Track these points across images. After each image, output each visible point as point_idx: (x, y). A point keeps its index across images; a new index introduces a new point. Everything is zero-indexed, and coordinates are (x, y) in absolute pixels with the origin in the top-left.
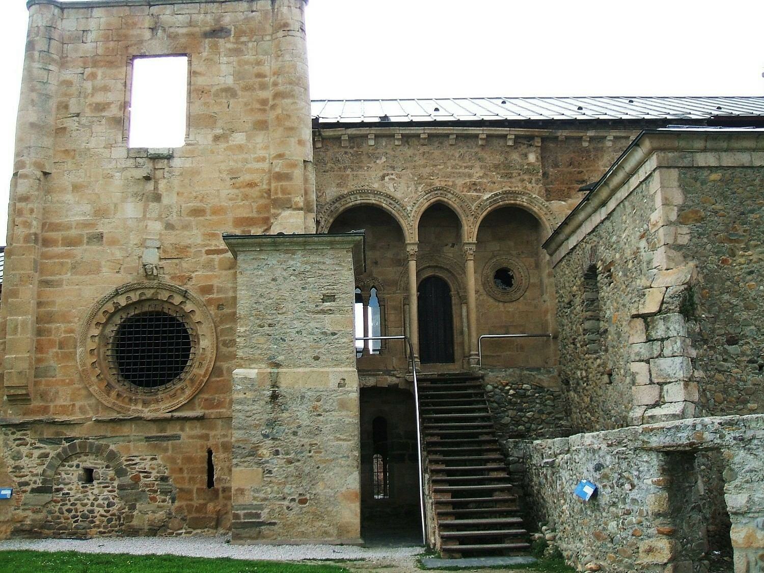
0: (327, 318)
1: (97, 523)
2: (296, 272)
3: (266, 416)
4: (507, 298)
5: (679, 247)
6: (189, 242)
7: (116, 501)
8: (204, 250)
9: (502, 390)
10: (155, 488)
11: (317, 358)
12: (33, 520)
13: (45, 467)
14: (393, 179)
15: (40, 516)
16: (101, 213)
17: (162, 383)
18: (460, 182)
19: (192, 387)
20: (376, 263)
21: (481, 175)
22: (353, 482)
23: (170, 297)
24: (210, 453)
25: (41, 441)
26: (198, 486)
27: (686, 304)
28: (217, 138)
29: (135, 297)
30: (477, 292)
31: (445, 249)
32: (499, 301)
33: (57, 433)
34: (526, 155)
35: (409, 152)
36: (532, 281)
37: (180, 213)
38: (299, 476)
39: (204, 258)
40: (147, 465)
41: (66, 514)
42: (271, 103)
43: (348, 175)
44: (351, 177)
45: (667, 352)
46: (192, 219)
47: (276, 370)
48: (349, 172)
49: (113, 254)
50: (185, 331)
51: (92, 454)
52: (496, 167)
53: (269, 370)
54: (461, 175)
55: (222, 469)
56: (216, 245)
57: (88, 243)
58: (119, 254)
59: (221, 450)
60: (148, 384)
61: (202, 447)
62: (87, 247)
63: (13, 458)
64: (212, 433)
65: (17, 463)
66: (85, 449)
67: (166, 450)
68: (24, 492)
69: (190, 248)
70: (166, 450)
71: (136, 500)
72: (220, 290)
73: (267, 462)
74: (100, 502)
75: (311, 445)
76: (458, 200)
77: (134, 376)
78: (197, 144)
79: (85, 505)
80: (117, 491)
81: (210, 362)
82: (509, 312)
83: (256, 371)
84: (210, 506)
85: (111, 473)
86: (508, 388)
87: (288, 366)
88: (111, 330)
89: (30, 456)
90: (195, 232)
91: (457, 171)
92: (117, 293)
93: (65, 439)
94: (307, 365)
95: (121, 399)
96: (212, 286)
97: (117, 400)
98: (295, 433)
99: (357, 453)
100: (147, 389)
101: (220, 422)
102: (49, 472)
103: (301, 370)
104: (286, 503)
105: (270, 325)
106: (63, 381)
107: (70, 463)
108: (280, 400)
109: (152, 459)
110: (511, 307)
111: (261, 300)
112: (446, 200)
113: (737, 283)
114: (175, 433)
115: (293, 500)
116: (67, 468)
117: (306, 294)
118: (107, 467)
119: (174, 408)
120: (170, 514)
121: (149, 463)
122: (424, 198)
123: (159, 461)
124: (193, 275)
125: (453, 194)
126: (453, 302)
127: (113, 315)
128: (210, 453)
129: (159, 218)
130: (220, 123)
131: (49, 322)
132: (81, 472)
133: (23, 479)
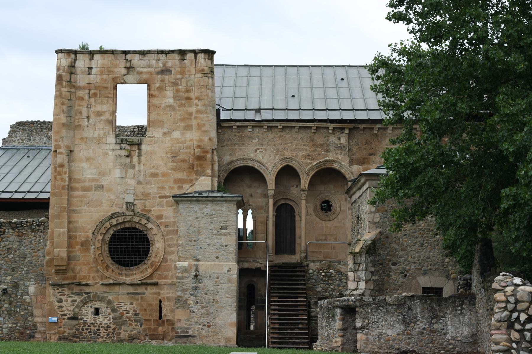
0: (223, 238)
1: (102, 336)
2: (208, 215)
3: (192, 285)
4: (327, 219)
5: (374, 223)
6: (150, 191)
7: (111, 325)
8: (158, 196)
9: (318, 273)
10: (132, 319)
11: (217, 258)
12: (69, 333)
13: (74, 307)
14: (262, 152)
15: (72, 331)
16: (102, 174)
17: (135, 265)
18: (300, 154)
20: (251, 196)
22: (233, 317)
23: (140, 220)
24: (160, 302)
25: (72, 293)
26: (154, 318)
27: (371, 249)
28: (164, 134)
29: (121, 220)
31: (292, 188)
33: (81, 290)
34: (339, 139)
35: (271, 135)
37: (145, 175)
38: (207, 314)
39: (158, 200)
40: (128, 307)
41: (85, 331)
42: (194, 115)
43: (236, 149)
44: (238, 150)
45: (361, 269)
46: (151, 179)
47: (197, 263)
48: (237, 147)
49: (109, 197)
50: (147, 238)
51: (99, 300)
53: (194, 263)
54: (301, 150)
55: (167, 310)
57: (95, 190)
58: (113, 197)
59: (166, 301)
60: (128, 266)
61: (156, 299)
63: (58, 302)
64: (162, 292)
65: (60, 304)
66: (96, 298)
67: (137, 300)
68: (64, 319)
70: (137, 300)
71: (122, 325)
73: (192, 307)
74: (103, 325)
75: (214, 300)
76: (298, 165)
77: (121, 261)
78: (154, 137)
79: (95, 327)
80: (112, 320)
83: (187, 263)
84: (160, 329)
85: (109, 310)
87: (203, 261)
88: (108, 237)
89: (66, 301)
90: (153, 186)
91: (299, 147)
92: (112, 217)
93: (85, 293)
94: (213, 261)
96: (162, 215)
98: (206, 294)
99: (235, 304)
100: (128, 268)
101: (166, 286)
102: (77, 310)
103: (209, 263)
104: (201, 326)
105: (195, 241)
106: (84, 263)
107: (87, 305)
108: (199, 277)
109: (130, 304)
110: (329, 224)
111: (191, 228)
112: (291, 164)
113: (399, 239)
115: (204, 325)
116: (86, 308)
117: (212, 226)
118: (107, 308)
120: (140, 332)
121: (128, 306)
123: (134, 305)
124: (152, 209)
127: (109, 229)
128: (160, 302)
129: (134, 178)
130: (166, 125)
131: (75, 232)
132: (93, 310)
133: (63, 313)
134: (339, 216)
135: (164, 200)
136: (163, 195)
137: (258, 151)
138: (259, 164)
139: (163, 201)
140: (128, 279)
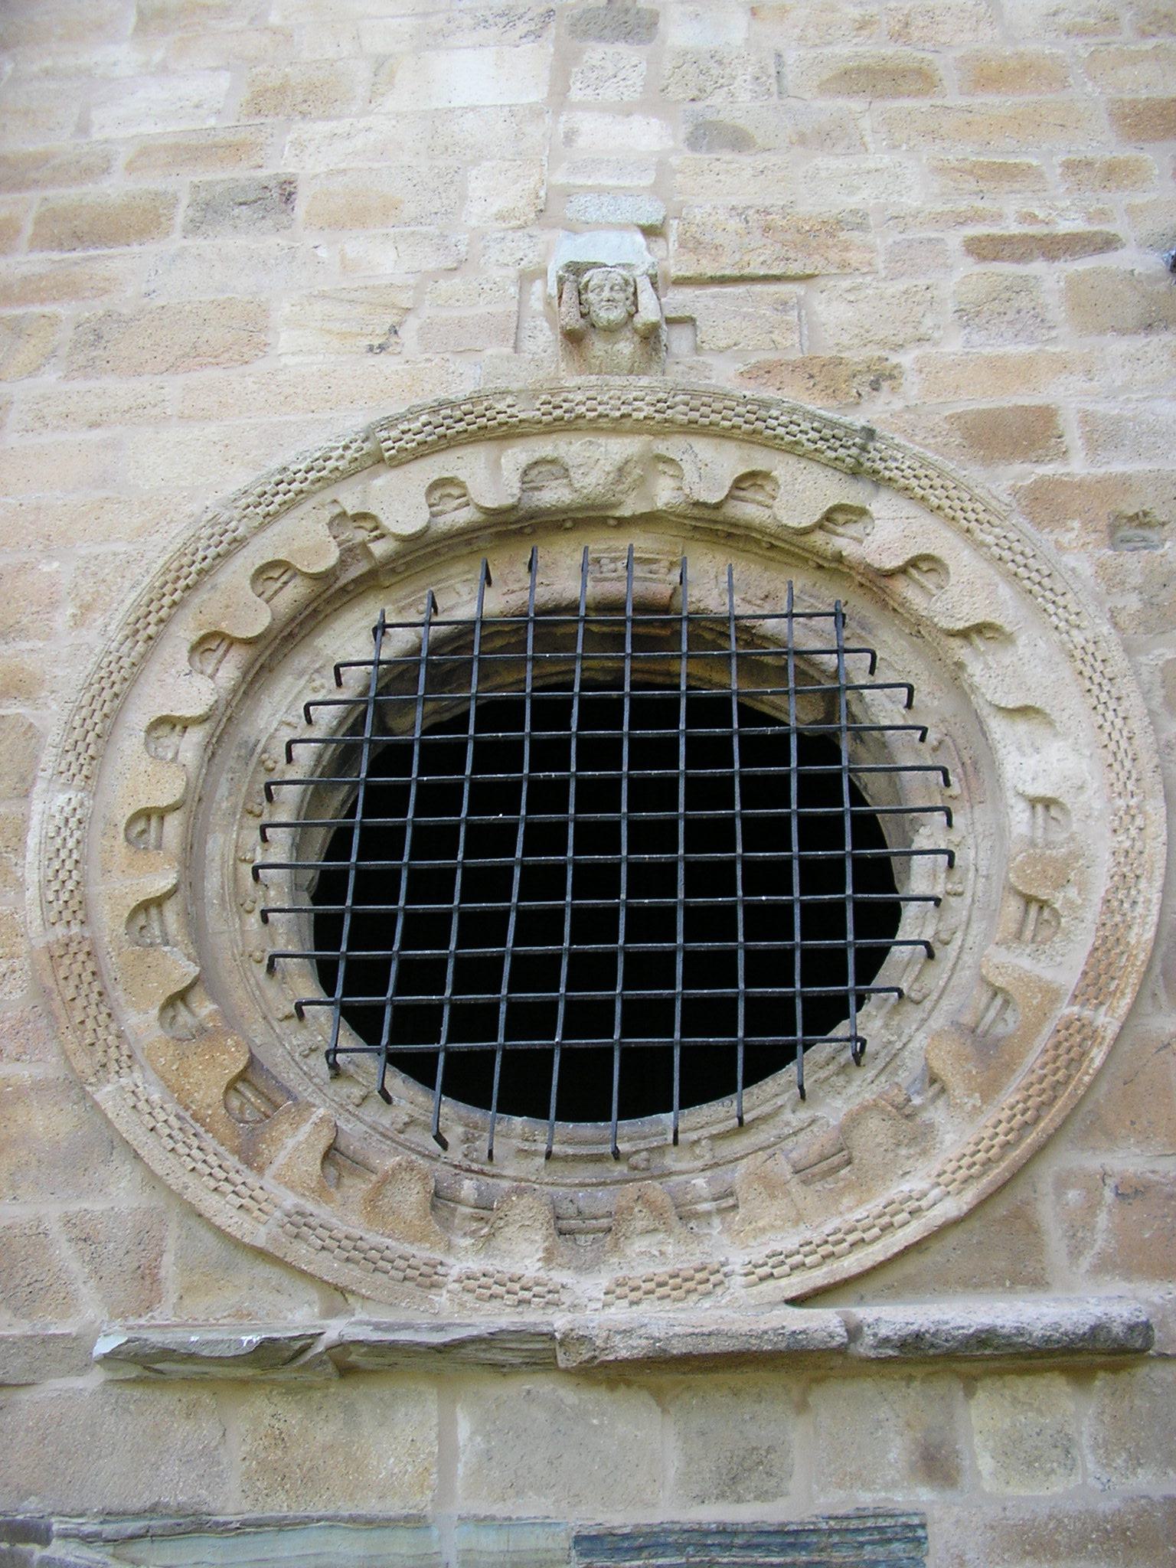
6: (853, 202)
19: (989, 1090)
29: (491, 479)
46: (856, 105)
56: (1032, 218)
57: (194, 227)
62: (185, 243)
69: (861, 227)
72: (1103, 436)
81: (1125, 880)
88: (300, 712)
95: (358, 1188)
97: (321, 1193)
114: (867, 1499)
119: (851, 1264)
124: (905, 360)
135: (1050, 276)
136: (1014, 229)
139: (1025, 286)
140: (591, 1286)
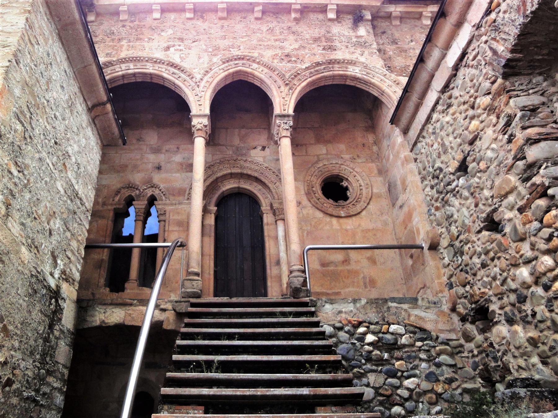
9: (351, 334)
20: (159, 168)
21: (297, 47)
30: (299, 203)
31: (253, 153)
32: (331, 215)
36: (375, 191)
43: (123, 45)
52: (316, 40)
54: (269, 47)
76: (266, 70)
82: (347, 230)
86: (361, 330)
91: (266, 44)
110: (350, 224)
112: (249, 70)
122: (221, 67)
125: (258, 63)
126: (265, 220)
134: (369, 207)
137: (172, 49)
138: (172, 70)
